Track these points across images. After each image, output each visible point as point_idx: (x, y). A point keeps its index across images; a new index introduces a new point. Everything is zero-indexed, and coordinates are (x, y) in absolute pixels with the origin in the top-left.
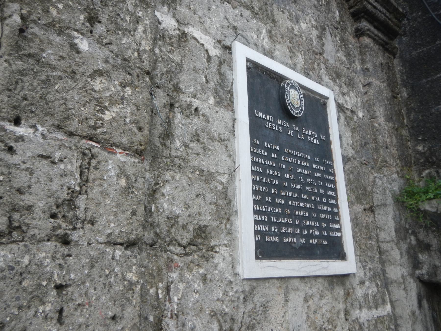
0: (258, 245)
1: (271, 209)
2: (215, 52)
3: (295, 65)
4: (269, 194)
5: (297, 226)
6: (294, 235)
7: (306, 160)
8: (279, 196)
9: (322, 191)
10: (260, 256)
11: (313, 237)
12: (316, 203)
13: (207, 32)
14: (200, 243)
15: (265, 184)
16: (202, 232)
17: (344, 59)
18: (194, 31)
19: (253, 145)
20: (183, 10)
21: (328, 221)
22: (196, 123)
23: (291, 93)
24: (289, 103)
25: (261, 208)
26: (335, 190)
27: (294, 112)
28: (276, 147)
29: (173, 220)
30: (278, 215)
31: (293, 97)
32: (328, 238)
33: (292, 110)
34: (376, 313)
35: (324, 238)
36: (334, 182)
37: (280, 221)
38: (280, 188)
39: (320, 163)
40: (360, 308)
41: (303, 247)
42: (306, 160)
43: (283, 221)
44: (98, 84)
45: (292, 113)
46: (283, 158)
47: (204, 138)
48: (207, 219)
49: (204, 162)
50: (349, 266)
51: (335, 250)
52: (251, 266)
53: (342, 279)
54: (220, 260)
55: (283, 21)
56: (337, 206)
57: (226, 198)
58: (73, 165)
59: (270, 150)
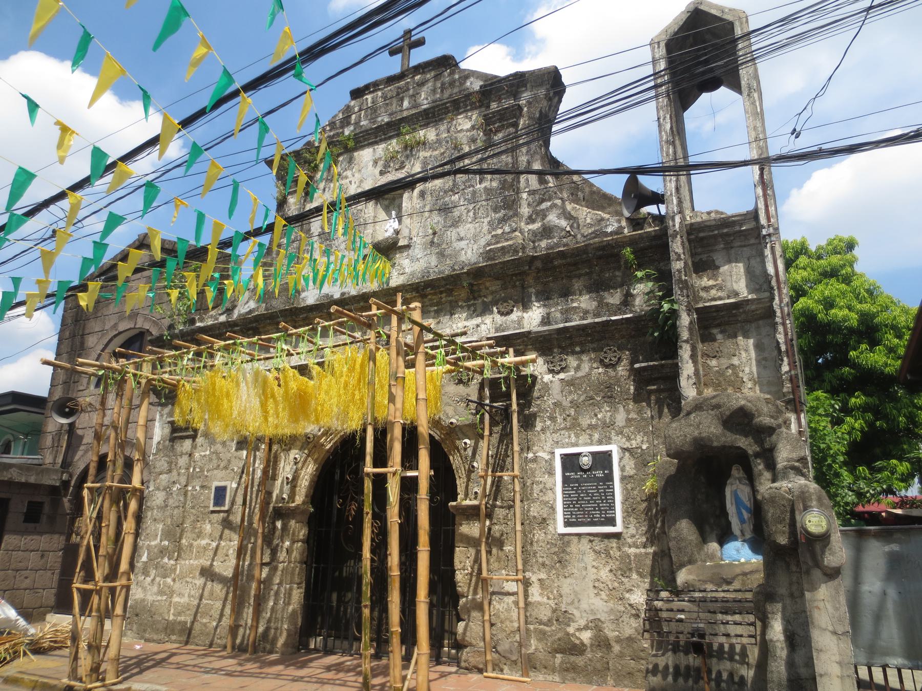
0: (565, 522)
3: (592, 441)
12: (598, 504)
13: (545, 451)
14: (543, 522)
16: (544, 519)
17: (635, 416)
18: (540, 454)
19: (563, 487)
20: (535, 448)
21: (606, 510)
22: (541, 486)
26: (613, 496)
29: (535, 517)
31: (586, 461)
32: (606, 518)
34: (638, 551)
36: (613, 492)
38: (577, 501)
39: (604, 485)
47: (544, 490)
48: (545, 516)
49: (546, 498)
50: (618, 528)
51: (612, 522)
52: (562, 529)
53: (617, 536)
54: (550, 528)
55: (585, 421)
56: (614, 503)
57: (553, 509)
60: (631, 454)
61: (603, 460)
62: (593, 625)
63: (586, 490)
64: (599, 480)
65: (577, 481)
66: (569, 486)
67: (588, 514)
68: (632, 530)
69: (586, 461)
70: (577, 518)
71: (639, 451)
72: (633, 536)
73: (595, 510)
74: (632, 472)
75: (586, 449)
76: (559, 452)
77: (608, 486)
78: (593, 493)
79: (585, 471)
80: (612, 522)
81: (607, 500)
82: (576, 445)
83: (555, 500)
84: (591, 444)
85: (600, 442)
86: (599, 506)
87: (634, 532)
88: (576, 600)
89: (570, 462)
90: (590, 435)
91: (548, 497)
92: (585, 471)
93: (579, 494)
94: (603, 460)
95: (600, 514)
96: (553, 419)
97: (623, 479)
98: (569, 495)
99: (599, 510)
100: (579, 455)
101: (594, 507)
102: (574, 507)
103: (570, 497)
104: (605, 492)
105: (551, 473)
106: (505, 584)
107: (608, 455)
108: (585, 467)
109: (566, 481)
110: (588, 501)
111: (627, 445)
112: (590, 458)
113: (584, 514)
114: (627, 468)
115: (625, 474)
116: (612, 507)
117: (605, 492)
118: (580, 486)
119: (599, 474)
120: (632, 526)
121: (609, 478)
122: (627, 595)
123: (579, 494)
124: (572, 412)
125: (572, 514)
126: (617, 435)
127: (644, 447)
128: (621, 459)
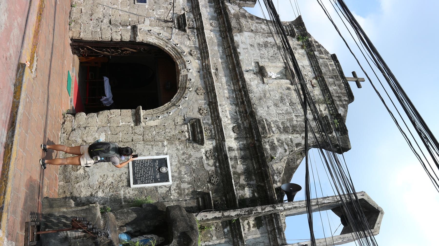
2: (165, 152)
13: (167, 150)
18: (166, 148)
19: (151, 160)
20: (169, 146)
21: (141, 180)
26: (148, 183)
29: (136, 146)
31: (164, 170)
32: (137, 180)
36: (149, 183)
39: (153, 179)
40: (124, 191)
44: (150, 134)
51: (135, 182)
53: (129, 185)
56: (144, 183)
58: (140, 133)
60: (168, 191)
61: (165, 177)
62: (87, 175)
63: (150, 170)
64: (155, 176)
65: (154, 166)
68: (131, 192)
69: (164, 170)
71: (170, 195)
72: (129, 193)
73: (140, 174)
74: (159, 191)
75: (170, 170)
76: (168, 157)
77: (152, 181)
79: (159, 169)
80: (135, 182)
82: (171, 165)
83: (145, 156)
84: (172, 172)
85: (173, 176)
87: (131, 193)
88: (97, 167)
89: (163, 162)
90: (176, 172)
91: (146, 152)
92: (159, 169)
93: (148, 167)
94: (165, 177)
95: (139, 177)
96: (184, 154)
97: (156, 187)
98: (147, 162)
100: (167, 166)
101: (142, 174)
102: (141, 165)
103: (146, 163)
104: (149, 179)
105: (158, 154)
106: (104, 133)
107: (167, 180)
108: (161, 170)
109: (154, 160)
111: (172, 189)
112: (165, 172)
114: (161, 189)
115: (158, 188)
116: (142, 182)
117: (149, 179)
119: (158, 176)
120: (134, 192)
121: (156, 181)
122: (101, 190)
123: (148, 167)
124: (187, 163)
125: (138, 164)
126: (177, 184)
127: (171, 197)
128: (165, 186)
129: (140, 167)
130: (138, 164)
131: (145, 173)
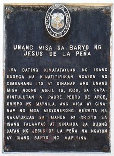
1: (24, 117)
4: (23, 106)
5: (51, 127)
6: (47, 134)
7: (70, 74)
8: (34, 106)
9: (87, 97)
10: (8, 150)
11: (69, 134)
12: (76, 108)
15: (20, 100)
21: (90, 122)
23: (53, 18)
24: (49, 29)
25: (13, 117)
27: (56, 35)
28: (34, 70)
30: (31, 121)
33: (52, 33)
35: (84, 134)
37: (33, 124)
38: (34, 101)
41: (55, 142)
42: (70, 74)
43: (36, 125)
45: (53, 36)
46: (41, 77)
59: (26, 74)
63: (54, 81)
65: (34, 62)
66: (19, 72)
67: (56, 128)
69: (57, 22)
70: (31, 135)
73: (68, 120)
77: (98, 74)
78: (66, 88)
81: (93, 101)
86: (76, 113)
93: (39, 88)
95: (79, 128)
98: (20, 88)
99: (77, 120)
101: (68, 115)
102: (27, 113)
103: (20, 93)
104: (90, 87)
110: (57, 101)
113: (47, 127)
118: (41, 72)
119: (83, 50)
123: (39, 88)
125: (22, 127)
129: (36, 120)
130: (22, 127)
131: (64, 100)
